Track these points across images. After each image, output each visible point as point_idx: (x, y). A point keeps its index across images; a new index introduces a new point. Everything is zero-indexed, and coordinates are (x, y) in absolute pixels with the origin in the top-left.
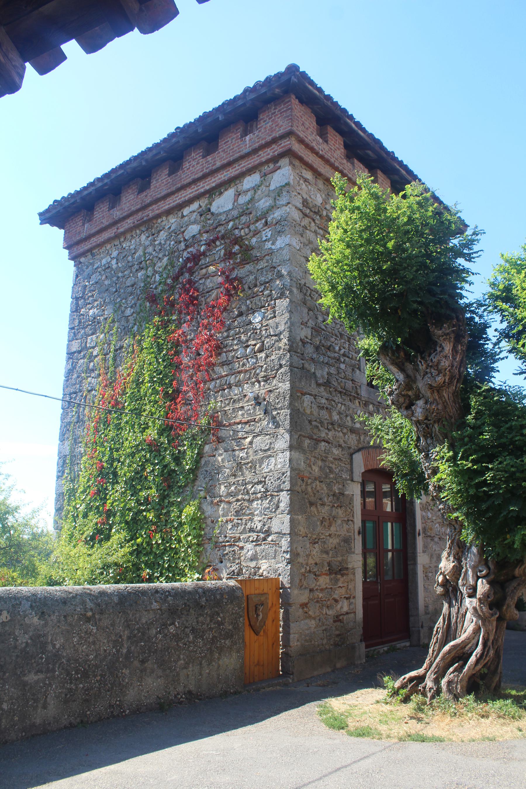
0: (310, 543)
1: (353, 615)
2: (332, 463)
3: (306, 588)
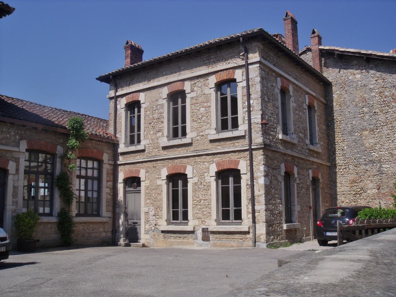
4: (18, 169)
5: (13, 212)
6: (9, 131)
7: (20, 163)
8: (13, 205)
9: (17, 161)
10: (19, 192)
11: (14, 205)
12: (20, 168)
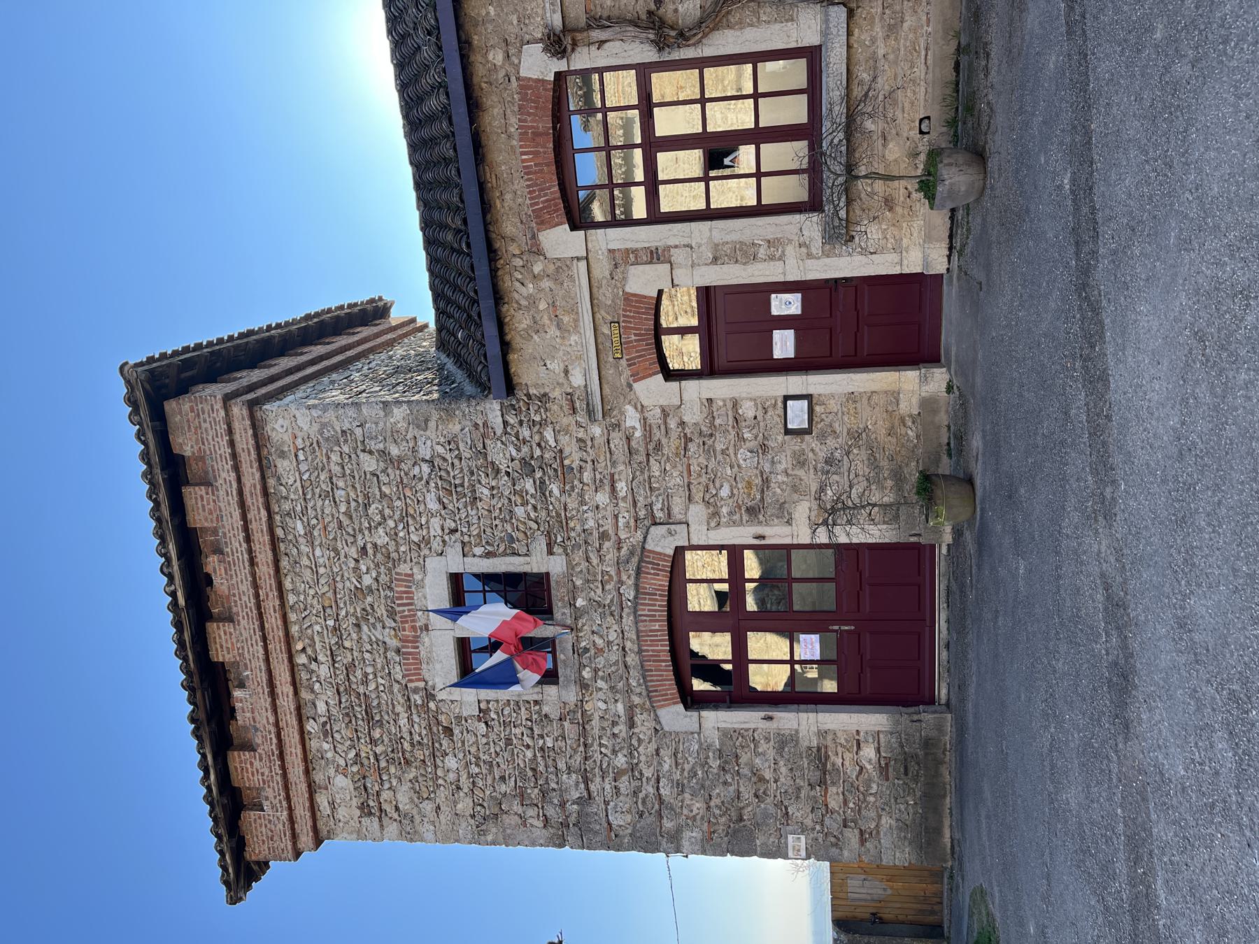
3: (841, 833)
6: (524, 303)
7: (629, 245)
9: (622, 259)
10: (728, 238)
11: (783, 252)
12: (647, 245)
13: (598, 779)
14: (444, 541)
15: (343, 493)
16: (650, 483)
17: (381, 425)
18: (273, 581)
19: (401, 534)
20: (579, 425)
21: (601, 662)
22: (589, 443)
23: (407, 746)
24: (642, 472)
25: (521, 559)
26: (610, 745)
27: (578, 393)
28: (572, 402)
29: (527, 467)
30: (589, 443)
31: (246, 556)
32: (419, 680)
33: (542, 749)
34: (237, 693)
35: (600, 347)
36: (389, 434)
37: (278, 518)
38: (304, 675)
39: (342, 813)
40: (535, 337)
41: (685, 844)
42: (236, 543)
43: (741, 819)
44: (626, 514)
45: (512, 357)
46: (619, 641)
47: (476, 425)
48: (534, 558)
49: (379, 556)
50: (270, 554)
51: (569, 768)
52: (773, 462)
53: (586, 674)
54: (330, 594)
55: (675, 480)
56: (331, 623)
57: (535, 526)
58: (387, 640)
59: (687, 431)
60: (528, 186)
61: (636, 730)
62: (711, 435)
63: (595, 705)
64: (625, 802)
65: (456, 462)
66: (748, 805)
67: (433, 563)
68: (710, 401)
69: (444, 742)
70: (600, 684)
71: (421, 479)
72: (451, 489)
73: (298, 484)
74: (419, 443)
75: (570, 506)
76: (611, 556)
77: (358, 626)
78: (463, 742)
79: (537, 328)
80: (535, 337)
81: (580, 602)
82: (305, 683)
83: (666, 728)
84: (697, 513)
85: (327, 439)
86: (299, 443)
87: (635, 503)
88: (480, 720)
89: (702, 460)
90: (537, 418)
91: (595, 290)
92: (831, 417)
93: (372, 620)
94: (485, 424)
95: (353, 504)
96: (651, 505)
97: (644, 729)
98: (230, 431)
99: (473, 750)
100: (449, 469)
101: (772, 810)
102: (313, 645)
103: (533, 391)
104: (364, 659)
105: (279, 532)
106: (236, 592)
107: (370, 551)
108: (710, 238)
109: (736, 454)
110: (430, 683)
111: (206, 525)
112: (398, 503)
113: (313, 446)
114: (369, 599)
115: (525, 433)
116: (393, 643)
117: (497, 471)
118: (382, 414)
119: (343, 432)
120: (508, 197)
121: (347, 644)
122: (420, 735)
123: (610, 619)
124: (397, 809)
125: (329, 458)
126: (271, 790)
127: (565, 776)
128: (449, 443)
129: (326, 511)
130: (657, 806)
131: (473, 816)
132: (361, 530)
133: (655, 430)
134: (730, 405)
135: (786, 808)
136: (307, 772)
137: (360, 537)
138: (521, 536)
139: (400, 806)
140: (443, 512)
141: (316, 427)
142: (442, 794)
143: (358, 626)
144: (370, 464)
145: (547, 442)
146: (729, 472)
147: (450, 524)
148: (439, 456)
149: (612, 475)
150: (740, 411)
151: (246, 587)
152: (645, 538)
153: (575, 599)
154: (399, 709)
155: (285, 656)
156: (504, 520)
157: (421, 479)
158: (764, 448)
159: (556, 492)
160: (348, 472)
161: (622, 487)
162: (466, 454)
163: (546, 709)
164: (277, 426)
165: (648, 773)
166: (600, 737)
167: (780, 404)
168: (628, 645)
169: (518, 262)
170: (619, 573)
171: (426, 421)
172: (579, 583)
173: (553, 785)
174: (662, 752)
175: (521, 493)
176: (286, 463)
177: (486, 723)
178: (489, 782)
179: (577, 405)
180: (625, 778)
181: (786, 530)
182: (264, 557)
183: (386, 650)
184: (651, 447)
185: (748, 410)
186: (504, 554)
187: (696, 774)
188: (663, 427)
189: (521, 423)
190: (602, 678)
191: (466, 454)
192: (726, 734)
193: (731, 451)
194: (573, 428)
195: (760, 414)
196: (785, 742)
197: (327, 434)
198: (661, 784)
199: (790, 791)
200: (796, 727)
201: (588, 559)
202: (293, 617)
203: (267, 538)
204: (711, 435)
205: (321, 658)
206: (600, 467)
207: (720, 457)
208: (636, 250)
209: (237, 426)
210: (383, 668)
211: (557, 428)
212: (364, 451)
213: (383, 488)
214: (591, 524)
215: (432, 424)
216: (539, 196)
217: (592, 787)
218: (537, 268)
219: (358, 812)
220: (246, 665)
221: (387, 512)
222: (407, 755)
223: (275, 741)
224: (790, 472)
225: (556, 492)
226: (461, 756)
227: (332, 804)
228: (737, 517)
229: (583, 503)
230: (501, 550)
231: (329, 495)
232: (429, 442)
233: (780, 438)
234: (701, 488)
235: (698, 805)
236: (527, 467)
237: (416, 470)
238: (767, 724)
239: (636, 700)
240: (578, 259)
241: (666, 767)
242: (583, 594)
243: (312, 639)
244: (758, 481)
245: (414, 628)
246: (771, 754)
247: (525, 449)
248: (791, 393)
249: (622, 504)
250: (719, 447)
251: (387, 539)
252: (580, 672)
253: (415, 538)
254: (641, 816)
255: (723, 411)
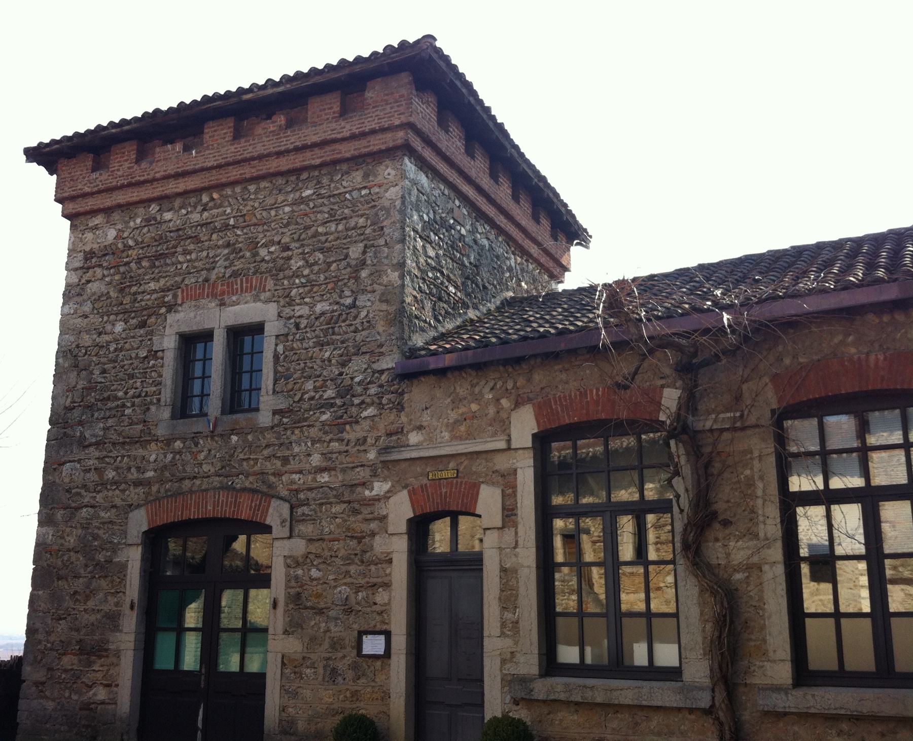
0: (52, 619)
1: (113, 706)
2: (99, 528)
4: (513, 510)
5: (504, 662)
6: (477, 390)
8: (503, 635)
10: (521, 584)
12: (519, 505)
13: (97, 454)
14: (290, 318)
15: (333, 229)
16: (326, 503)
17: (386, 261)
18: (264, 171)
19: (297, 281)
20: (377, 439)
21: (187, 457)
22: (362, 448)
23: (134, 289)
24: (335, 496)
25: (271, 387)
26: (123, 465)
27: (404, 438)
28: (397, 433)
29: (346, 391)
30: (362, 448)
31: (283, 148)
32: (183, 299)
33: (124, 406)
34: (179, 147)
35: (439, 460)
36: (378, 268)
37: (316, 173)
38: (193, 200)
39: (89, 236)
40: (449, 400)
41: (44, 530)
42: (294, 138)
43: (59, 579)
44: (302, 481)
45: (432, 379)
46: (202, 474)
47: (381, 346)
48: (271, 397)
49: (282, 262)
50: (285, 168)
51: (108, 428)
52: (337, 619)
53: (178, 444)
54: (254, 221)
55: (328, 527)
56: (232, 222)
57: (297, 398)
58: (216, 270)
59: (367, 540)
60: (570, 396)
61: (132, 488)
62: (362, 562)
63: (153, 453)
64: (78, 477)
65: (352, 328)
66: (69, 586)
67: (272, 309)
68: (390, 561)
69: (135, 321)
70: (170, 457)
71: (341, 297)
72: (332, 321)
73: (343, 190)
74: (369, 295)
75: (312, 430)
76: (269, 467)
77: (228, 245)
78: (133, 337)
79: (457, 402)
80: (449, 400)
81: (234, 438)
82: (187, 202)
83: (131, 515)
84: (298, 546)
85: (376, 214)
86: (377, 190)
87: (310, 489)
88: (149, 351)
89: (342, 553)
90: (384, 401)
91: (484, 456)
92: (371, 675)
93: (232, 257)
94: (382, 354)
95: (323, 238)
96: (308, 505)
97: (132, 495)
98: (383, 130)
99: (127, 346)
100: (348, 322)
101: (66, 605)
102: (216, 207)
103: (406, 396)
104: (202, 251)
105: (304, 176)
106: (256, 141)
107: (285, 254)
108: (523, 566)
109: (345, 584)
110: (180, 308)
111: (310, 113)
112: (322, 277)
113: (371, 201)
114: (248, 254)
115: (373, 390)
116: (213, 277)
117: (343, 365)
118: (395, 261)
119: (382, 228)
120: (564, 376)
121: (214, 236)
122: (142, 300)
123: (219, 465)
124: (88, 282)
125: (362, 216)
126: (106, 177)
127: (102, 425)
128: (368, 322)
129: (319, 215)
130: (73, 505)
131: (78, 346)
132: (302, 245)
133: (369, 509)
134: (386, 580)
135: (65, 618)
136: (119, 206)
137: (297, 245)
138: (290, 386)
139: (90, 285)
140: (313, 317)
141: (387, 204)
142: (95, 319)
143: (228, 245)
144: (355, 252)
145: (365, 409)
146: (331, 577)
147: (304, 323)
148: (359, 313)
149: (334, 469)
150: (381, 589)
151: (260, 149)
152: (281, 499)
153: (237, 434)
154: (162, 282)
155: (206, 184)
156: (303, 370)
157: (341, 297)
158: (349, 611)
159: (324, 417)
160: (350, 233)
161: (324, 478)
162: (359, 337)
163: (153, 409)
164: (389, 170)
165: (99, 498)
166: (129, 456)
167: (384, 627)
168: (198, 482)
169: (510, 385)
170: (256, 474)
171: (387, 301)
172: (250, 437)
173: (96, 415)
174: (114, 511)
175: (324, 386)
176: (359, 179)
177: (146, 357)
178: (102, 360)
179: (394, 438)
180: (96, 478)
181: (280, 629)
182: (284, 164)
183: (208, 270)
184: (356, 506)
185: (381, 597)
186: (276, 372)
187: (95, 539)
188: (371, 516)
189: (381, 386)
190: (173, 458)
191: (359, 337)
192: (123, 568)
193: (348, 580)
194: (375, 434)
195: (378, 608)
196: (113, 620)
197: (381, 213)
198: (90, 509)
199: (77, 623)
200: (125, 631)
201: (267, 446)
202: (238, 189)
203: (298, 165)
204: (362, 562)
205: (206, 214)
206: (342, 458)
207: (344, 568)
208: (515, 496)
209: (389, 135)
210: (195, 267)
211: (377, 419)
212: (366, 247)
213: (334, 265)
214: (296, 449)
215: (384, 307)
216: (562, 405)
217: (92, 449)
218: (505, 403)
219: (88, 249)
220: (200, 152)
221: (316, 268)
222: (127, 290)
223: (142, 179)
224: (328, 634)
225: (324, 417)
226: (123, 336)
227: (96, 228)
228: (293, 584)
229: (314, 442)
230: (279, 368)
231: (333, 217)
232: (369, 304)
233: (356, 626)
234: (319, 551)
235: (72, 541)
236: (346, 391)
237: (347, 293)
238: (128, 605)
239: (154, 489)
240: (509, 441)
241: (102, 514)
242: (241, 442)
243: (221, 206)
244: (322, 605)
245: (223, 293)
246: (106, 608)
247: (359, 389)
248: (394, 639)
249: (310, 477)
250: (352, 569)
251: (294, 268)
252: (179, 439)
253: (294, 292)
254: (67, 491)
255: (381, 573)
